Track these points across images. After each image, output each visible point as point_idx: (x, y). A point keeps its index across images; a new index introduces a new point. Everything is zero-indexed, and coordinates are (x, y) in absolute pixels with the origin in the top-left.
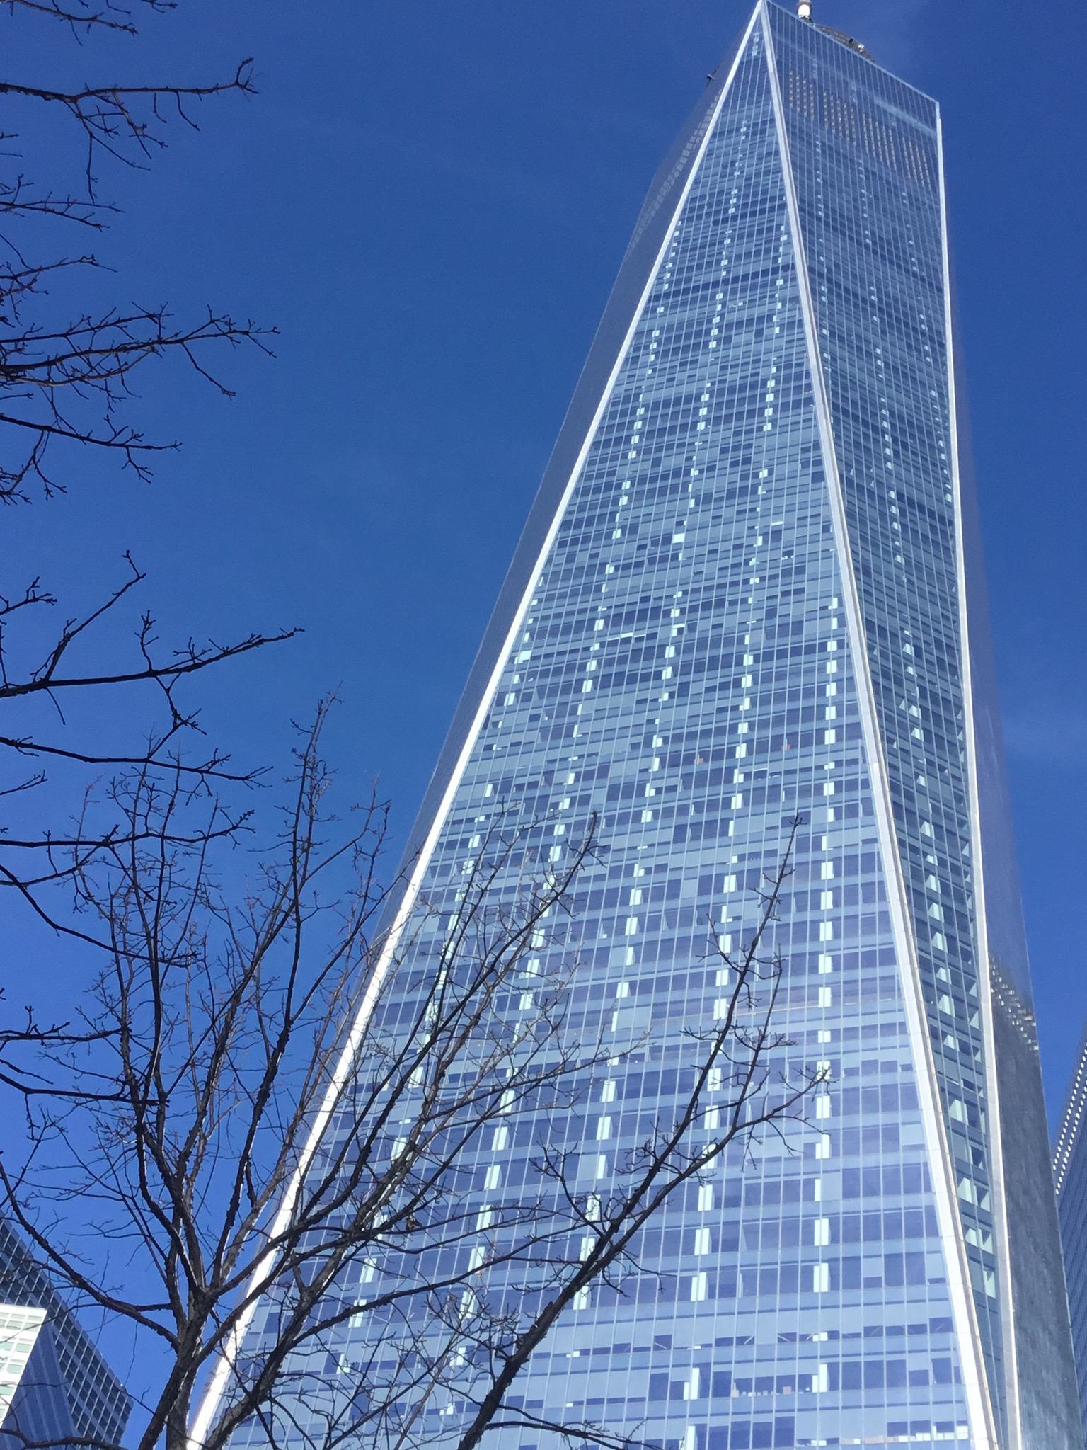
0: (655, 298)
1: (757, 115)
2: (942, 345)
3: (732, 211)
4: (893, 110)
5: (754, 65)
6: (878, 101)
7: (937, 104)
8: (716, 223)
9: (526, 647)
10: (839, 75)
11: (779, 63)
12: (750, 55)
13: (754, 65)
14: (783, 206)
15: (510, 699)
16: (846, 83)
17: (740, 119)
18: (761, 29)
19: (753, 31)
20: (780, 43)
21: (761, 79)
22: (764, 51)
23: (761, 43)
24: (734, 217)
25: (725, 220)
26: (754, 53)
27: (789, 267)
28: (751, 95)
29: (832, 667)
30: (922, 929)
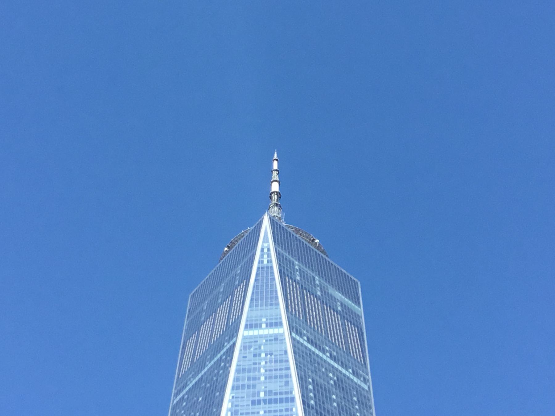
1: (271, 315)
3: (262, 395)
4: (338, 295)
5: (265, 270)
7: (359, 283)
8: (253, 403)
11: (280, 271)
12: (262, 262)
13: (265, 270)
14: (293, 400)
16: (314, 278)
17: (262, 316)
18: (268, 242)
19: (263, 242)
20: (279, 254)
21: (272, 285)
22: (271, 262)
24: (265, 401)
25: (259, 402)
26: (265, 262)
28: (267, 298)
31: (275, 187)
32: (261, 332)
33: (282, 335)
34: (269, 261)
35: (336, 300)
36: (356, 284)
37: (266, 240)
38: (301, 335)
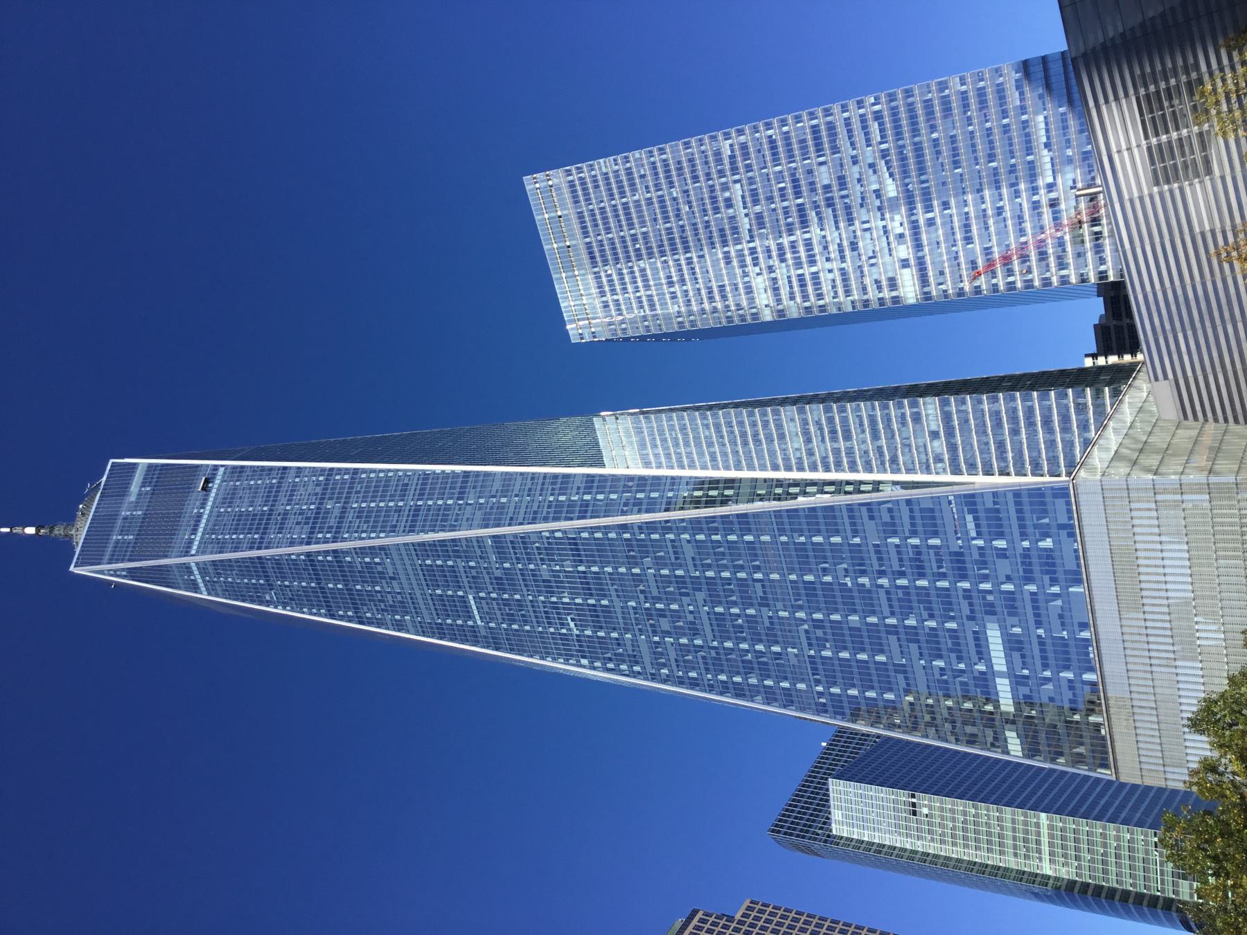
0: (332, 616)
2: (331, 469)
4: (134, 488)
5: (132, 573)
6: (133, 498)
7: (111, 461)
9: (578, 661)
10: (119, 522)
11: (130, 560)
13: (132, 573)
14: (259, 558)
15: (611, 665)
16: (125, 518)
23: (115, 571)
27: (308, 554)
29: (585, 535)
30: (724, 502)
31: (30, 530)
32: (200, 581)
33: (197, 564)
34: (123, 570)
35: (140, 494)
36: (114, 465)
37: (101, 572)
38: (191, 542)
